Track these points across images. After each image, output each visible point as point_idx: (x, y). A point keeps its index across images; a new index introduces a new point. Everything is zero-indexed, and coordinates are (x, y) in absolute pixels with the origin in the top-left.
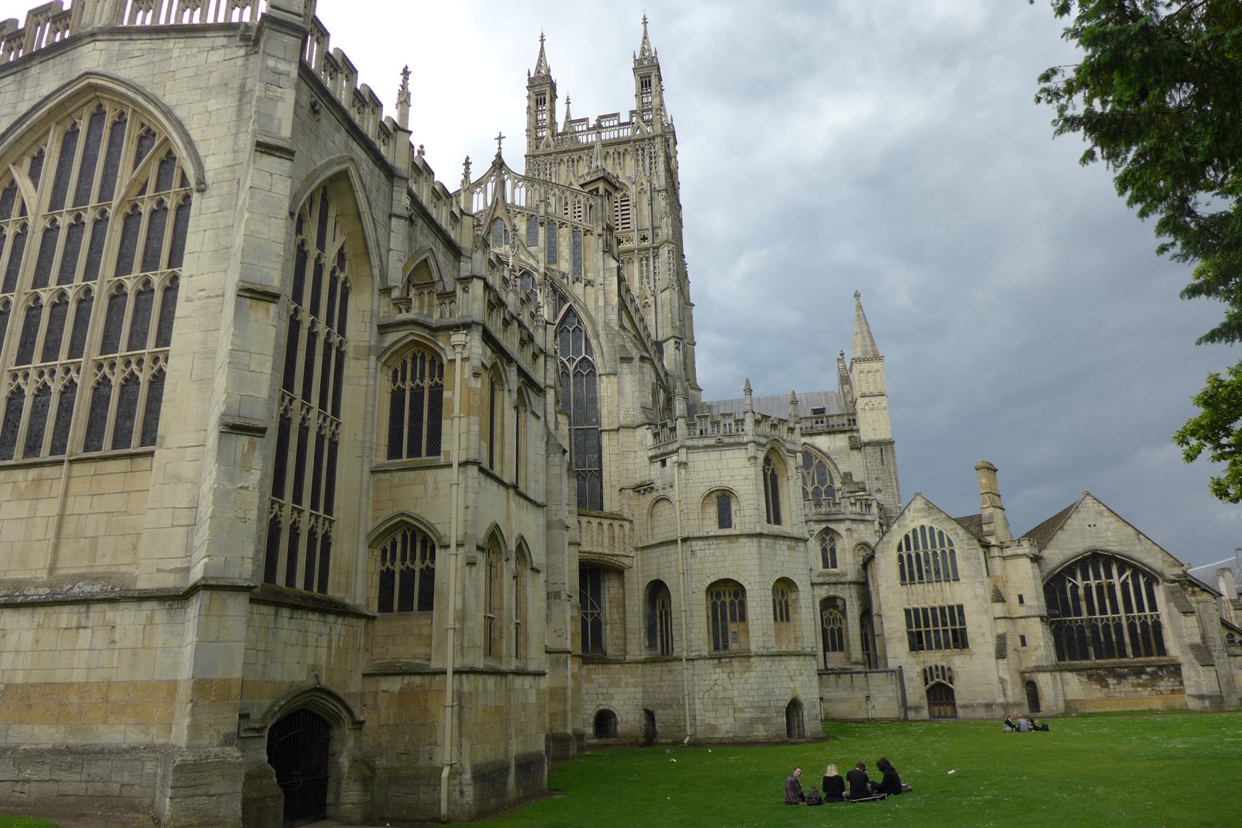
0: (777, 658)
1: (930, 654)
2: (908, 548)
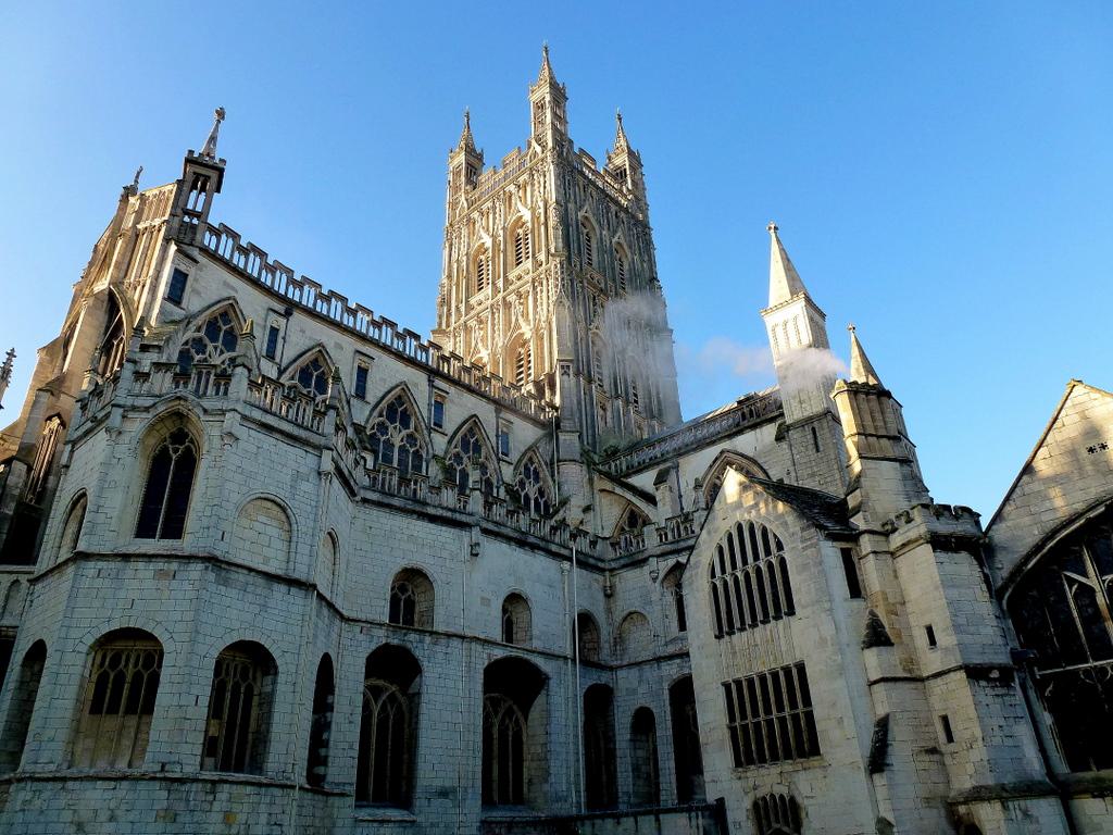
0: (50, 785)
1: (763, 771)
2: (723, 571)
